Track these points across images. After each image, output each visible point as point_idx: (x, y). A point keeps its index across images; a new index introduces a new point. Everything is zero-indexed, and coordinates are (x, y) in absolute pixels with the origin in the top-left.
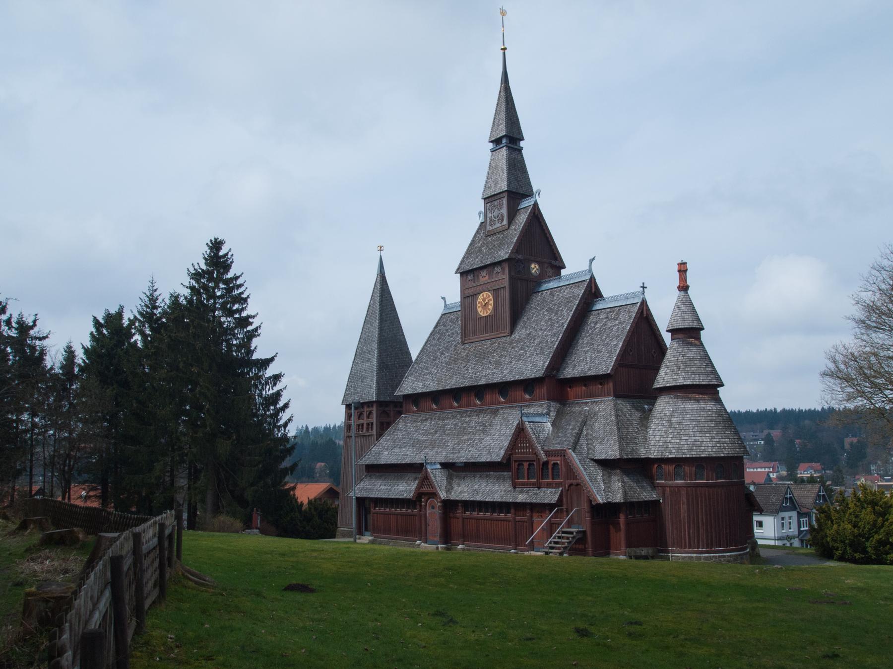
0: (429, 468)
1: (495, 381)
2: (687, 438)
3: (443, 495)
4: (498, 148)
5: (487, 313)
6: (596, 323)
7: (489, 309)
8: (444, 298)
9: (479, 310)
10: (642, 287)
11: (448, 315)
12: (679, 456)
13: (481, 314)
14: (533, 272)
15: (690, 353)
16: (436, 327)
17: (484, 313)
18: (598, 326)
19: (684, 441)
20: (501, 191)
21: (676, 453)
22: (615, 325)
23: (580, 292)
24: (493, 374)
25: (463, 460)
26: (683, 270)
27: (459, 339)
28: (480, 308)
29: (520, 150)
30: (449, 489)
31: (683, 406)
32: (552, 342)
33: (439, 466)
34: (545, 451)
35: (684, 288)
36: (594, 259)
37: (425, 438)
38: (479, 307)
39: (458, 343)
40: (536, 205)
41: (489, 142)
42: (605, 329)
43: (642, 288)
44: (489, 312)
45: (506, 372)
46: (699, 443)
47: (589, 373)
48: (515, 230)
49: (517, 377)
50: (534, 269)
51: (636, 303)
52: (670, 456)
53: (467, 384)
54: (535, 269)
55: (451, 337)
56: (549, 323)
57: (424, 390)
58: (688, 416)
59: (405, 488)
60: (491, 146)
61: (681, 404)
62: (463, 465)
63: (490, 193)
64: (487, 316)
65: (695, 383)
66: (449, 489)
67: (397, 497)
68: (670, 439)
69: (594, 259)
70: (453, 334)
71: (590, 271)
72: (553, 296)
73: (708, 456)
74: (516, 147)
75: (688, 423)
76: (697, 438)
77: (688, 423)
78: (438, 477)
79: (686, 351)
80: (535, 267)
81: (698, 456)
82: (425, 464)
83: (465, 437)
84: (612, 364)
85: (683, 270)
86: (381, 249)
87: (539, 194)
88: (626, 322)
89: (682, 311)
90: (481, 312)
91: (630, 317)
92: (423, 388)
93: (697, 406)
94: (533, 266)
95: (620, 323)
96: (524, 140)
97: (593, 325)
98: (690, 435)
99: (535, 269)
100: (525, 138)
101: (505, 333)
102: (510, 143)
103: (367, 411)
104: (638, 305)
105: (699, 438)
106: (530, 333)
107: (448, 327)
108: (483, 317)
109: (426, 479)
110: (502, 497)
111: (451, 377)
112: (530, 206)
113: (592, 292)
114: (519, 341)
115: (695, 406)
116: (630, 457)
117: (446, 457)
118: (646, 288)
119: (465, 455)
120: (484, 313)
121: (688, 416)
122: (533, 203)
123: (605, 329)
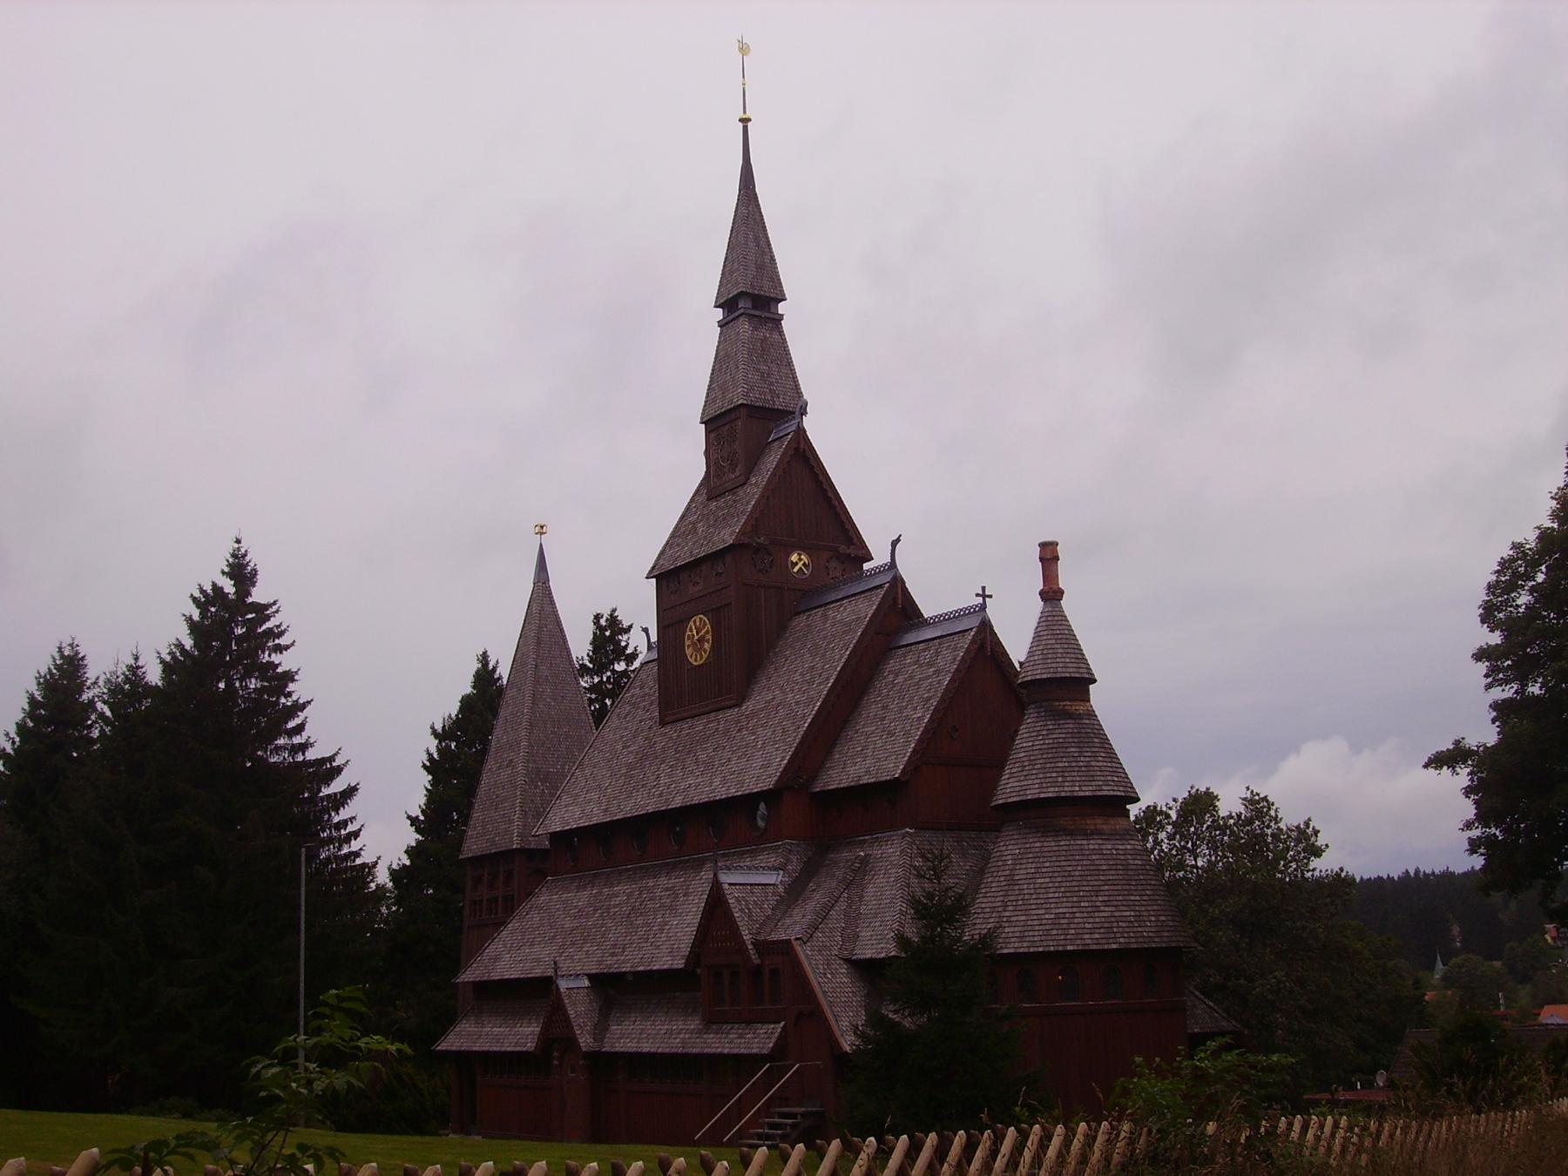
0: (563, 985)
3: (585, 1041)
10: (977, 595)
12: (1022, 950)
14: (796, 570)
18: (900, 679)
19: (1035, 917)
26: (1049, 555)
30: (600, 1030)
31: (1038, 845)
33: (586, 983)
35: (1051, 595)
36: (898, 540)
43: (980, 600)
50: (796, 563)
51: (968, 630)
54: (800, 565)
58: (1047, 864)
59: (521, 1035)
63: (713, 413)
64: (702, 665)
65: (1063, 794)
66: (600, 1030)
69: (898, 540)
76: (1061, 910)
77: (1047, 880)
79: (1051, 727)
81: (1061, 948)
82: (554, 978)
84: (906, 758)
85: (1049, 555)
86: (541, 530)
89: (1044, 643)
92: (580, 818)
93: (1068, 843)
94: (794, 558)
98: (1048, 906)
99: (800, 565)
101: (731, 699)
112: (789, 434)
114: (754, 714)
117: (600, 962)
118: (990, 596)
119: (632, 961)
122: (794, 428)
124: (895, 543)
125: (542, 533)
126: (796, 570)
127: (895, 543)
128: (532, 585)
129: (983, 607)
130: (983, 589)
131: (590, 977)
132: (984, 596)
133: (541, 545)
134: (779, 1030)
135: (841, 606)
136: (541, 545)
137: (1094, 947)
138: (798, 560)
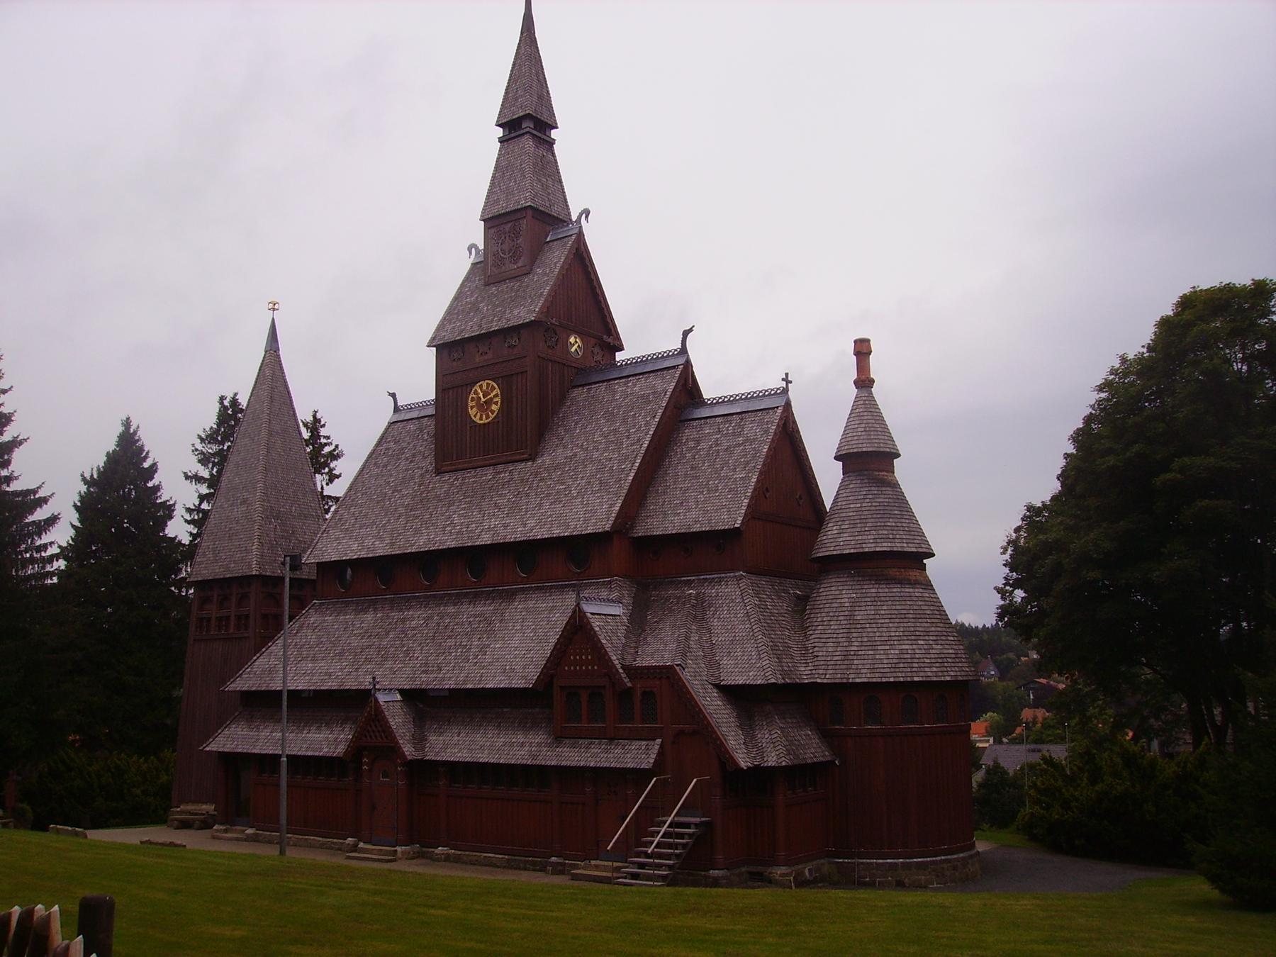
1: (511, 538)
2: (888, 647)
3: (408, 750)
4: (513, 135)
5: (487, 417)
6: (698, 442)
7: (493, 412)
8: (393, 395)
9: (472, 412)
10: (783, 380)
11: (400, 425)
13: (477, 420)
14: (573, 350)
15: (883, 496)
16: (379, 443)
17: (481, 419)
18: (703, 445)
19: (882, 652)
20: (519, 207)
21: (868, 675)
22: (739, 445)
23: (668, 385)
24: (505, 526)
25: (450, 684)
27: (429, 463)
28: (475, 409)
29: (550, 143)
30: (419, 741)
31: (873, 590)
32: (623, 470)
33: (399, 697)
34: (623, 667)
35: (864, 382)
36: (691, 330)
37: (365, 642)
38: (472, 407)
39: (427, 471)
40: (580, 235)
41: (497, 125)
42: (718, 451)
44: (492, 416)
45: (531, 523)
46: (909, 656)
47: (696, 528)
48: (544, 274)
49: (556, 532)
50: (574, 345)
51: (774, 408)
52: (858, 680)
53: (453, 544)
54: (576, 346)
55: (411, 462)
56: (611, 438)
57: (363, 554)
58: (885, 608)
60: (500, 132)
61: (871, 586)
62: (447, 694)
66: (419, 741)
67: (309, 753)
68: (855, 648)
69: (691, 330)
70: (414, 455)
71: (683, 350)
72: (615, 392)
73: (924, 679)
74: (543, 137)
75: (887, 621)
76: (904, 647)
77: (887, 621)
78: (398, 719)
79: (876, 492)
80: (576, 342)
81: (909, 679)
83: (451, 642)
87: (587, 217)
88: (761, 439)
89: (865, 422)
90: (475, 416)
91: (766, 431)
92: (360, 550)
93: (899, 590)
94: (572, 340)
95: (745, 441)
96: (557, 128)
97: (692, 444)
98: (892, 642)
99: (576, 346)
100: (559, 125)
101: (523, 454)
102: (535, 129)
103: (237, 594)
104: (780, 411)
105: (907, 647)
106: (575, 455)
107: (404, 445)
108: (480, 425)
109: (377, 717)
110: (535, 757)
111: (417, 532)
112: (571, 235)
113: (688, 389)
115: (895, 590)
116: (788, 681)
119: (452, 677)
120: (481, 419)
121: (885, 608)
123: (718, 451)
124: (686, 334)
125: (274, 310)
126: (573, 350)
127: (686, 334)
128: (264, 353)
129: (786, 391)
130: (787, 375)
131: (402, 692)
132: (787, 380)
133: (273, 319)
134: (657, 747)
135: (628, 382)
136: (273, 319)
137: (935, 679)
138: (575, 343)
